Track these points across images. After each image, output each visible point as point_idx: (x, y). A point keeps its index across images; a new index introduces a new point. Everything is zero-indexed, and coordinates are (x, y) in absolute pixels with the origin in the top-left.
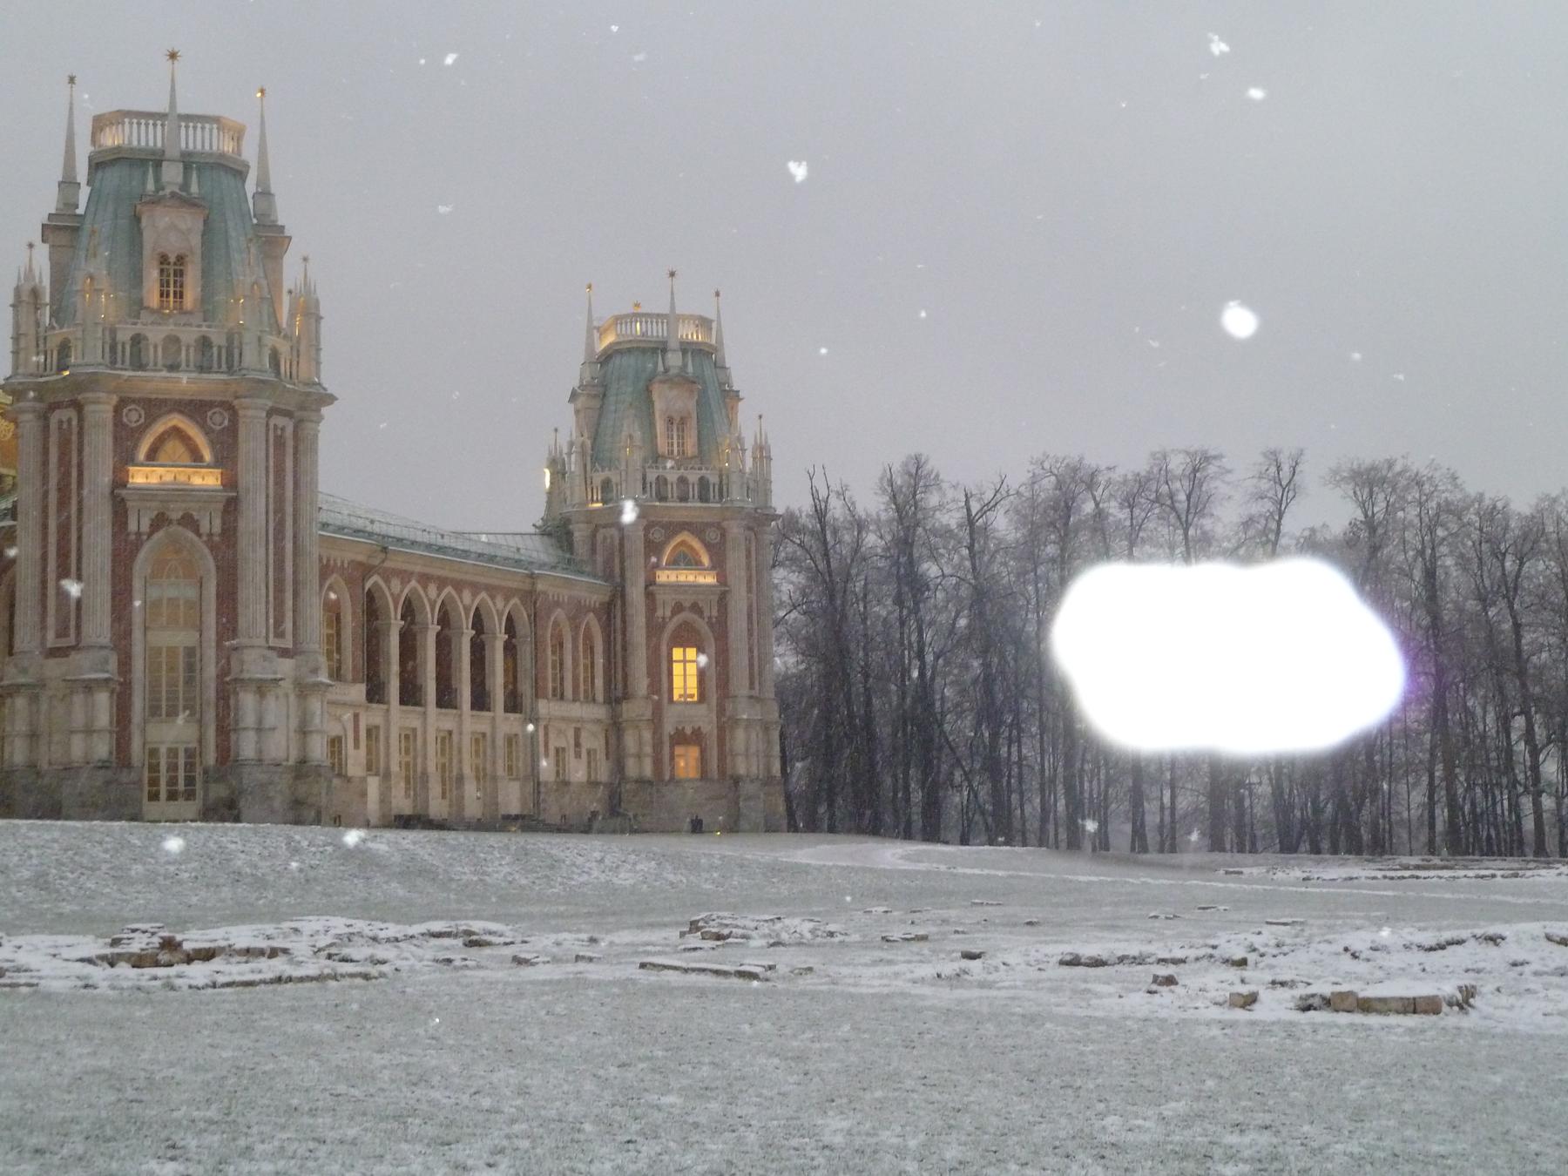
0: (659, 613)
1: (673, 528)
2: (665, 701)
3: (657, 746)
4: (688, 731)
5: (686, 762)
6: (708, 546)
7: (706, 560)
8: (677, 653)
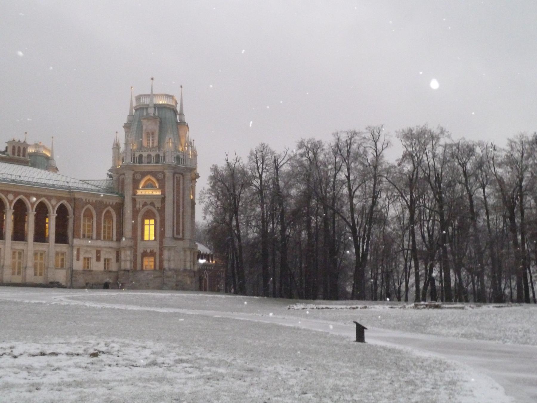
0: (137, 206)
1: (144, 174)
2: (139, 238)
3: (135, 256)
4: (148, 251)
5: (149, 263)
6: (158, 180)
7: (157, 186)
8: (146, 222)
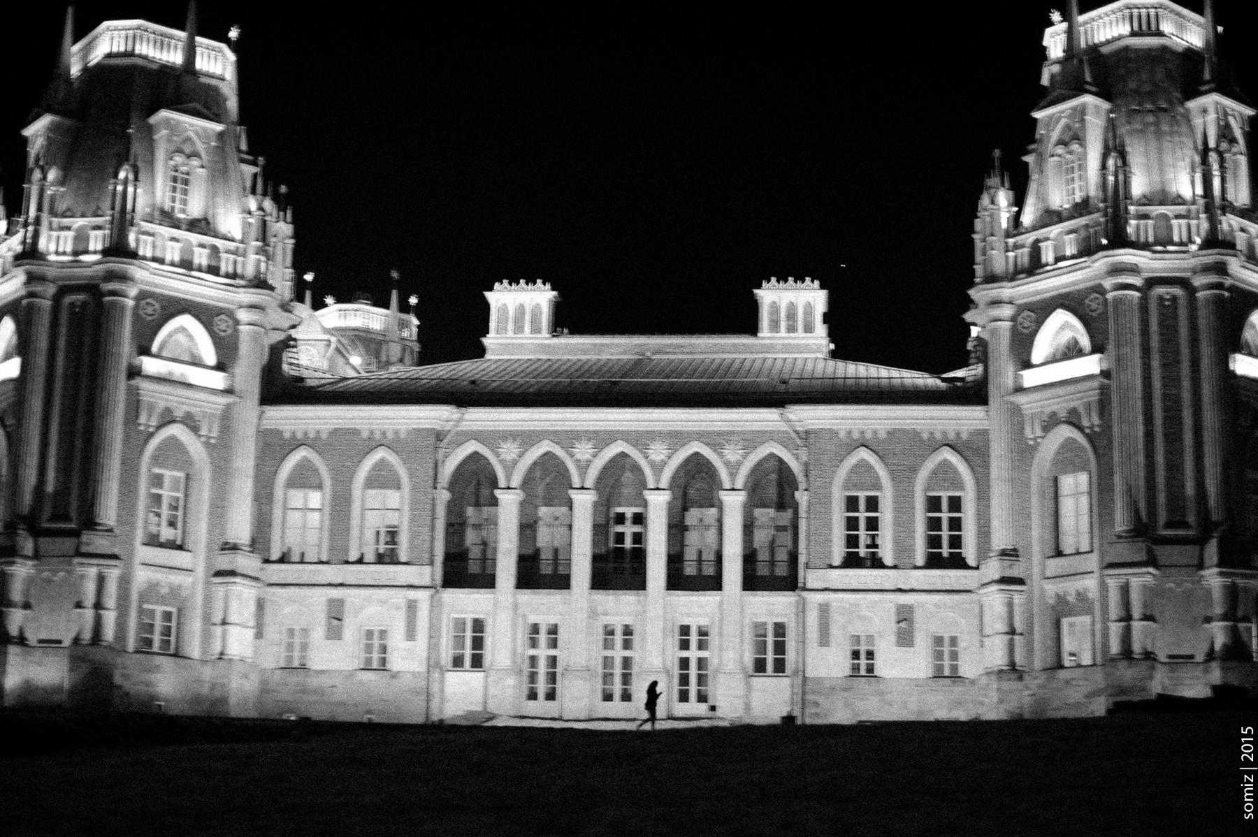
0: (1028, 433)
